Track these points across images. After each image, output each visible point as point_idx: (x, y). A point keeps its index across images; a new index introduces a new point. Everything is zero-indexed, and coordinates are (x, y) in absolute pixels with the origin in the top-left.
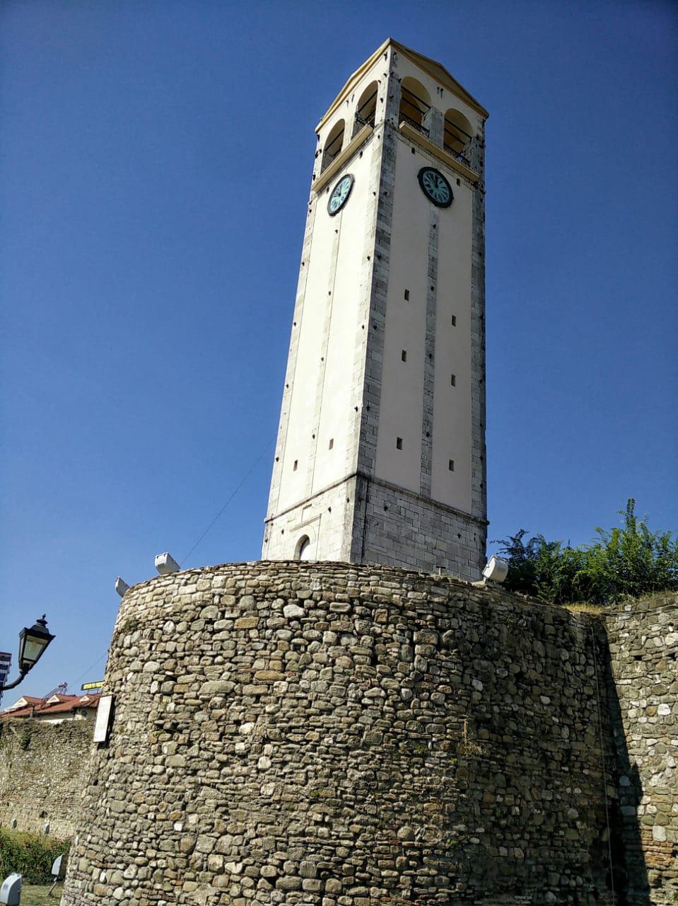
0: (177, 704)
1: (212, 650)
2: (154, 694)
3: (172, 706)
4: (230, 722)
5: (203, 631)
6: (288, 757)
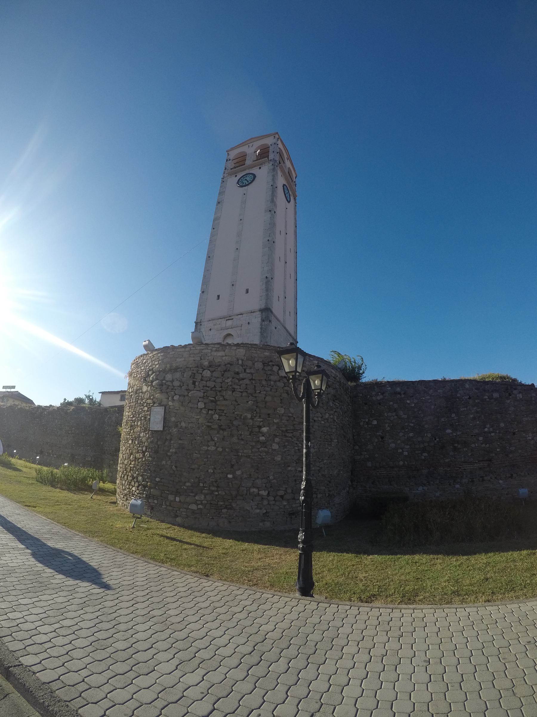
0: (220, 416)
1: (240, 389)
2: (201, 409)
3: (216, 416)
4: (255, 426)
5: (233, 378)
6: (287, 444)
